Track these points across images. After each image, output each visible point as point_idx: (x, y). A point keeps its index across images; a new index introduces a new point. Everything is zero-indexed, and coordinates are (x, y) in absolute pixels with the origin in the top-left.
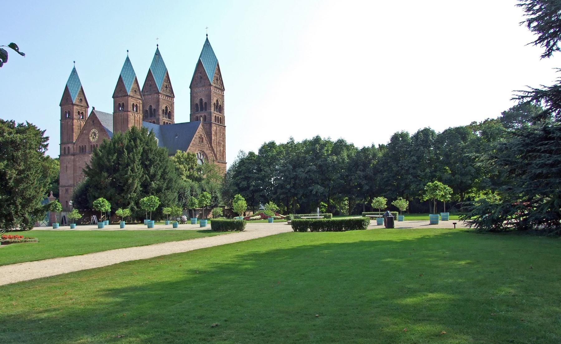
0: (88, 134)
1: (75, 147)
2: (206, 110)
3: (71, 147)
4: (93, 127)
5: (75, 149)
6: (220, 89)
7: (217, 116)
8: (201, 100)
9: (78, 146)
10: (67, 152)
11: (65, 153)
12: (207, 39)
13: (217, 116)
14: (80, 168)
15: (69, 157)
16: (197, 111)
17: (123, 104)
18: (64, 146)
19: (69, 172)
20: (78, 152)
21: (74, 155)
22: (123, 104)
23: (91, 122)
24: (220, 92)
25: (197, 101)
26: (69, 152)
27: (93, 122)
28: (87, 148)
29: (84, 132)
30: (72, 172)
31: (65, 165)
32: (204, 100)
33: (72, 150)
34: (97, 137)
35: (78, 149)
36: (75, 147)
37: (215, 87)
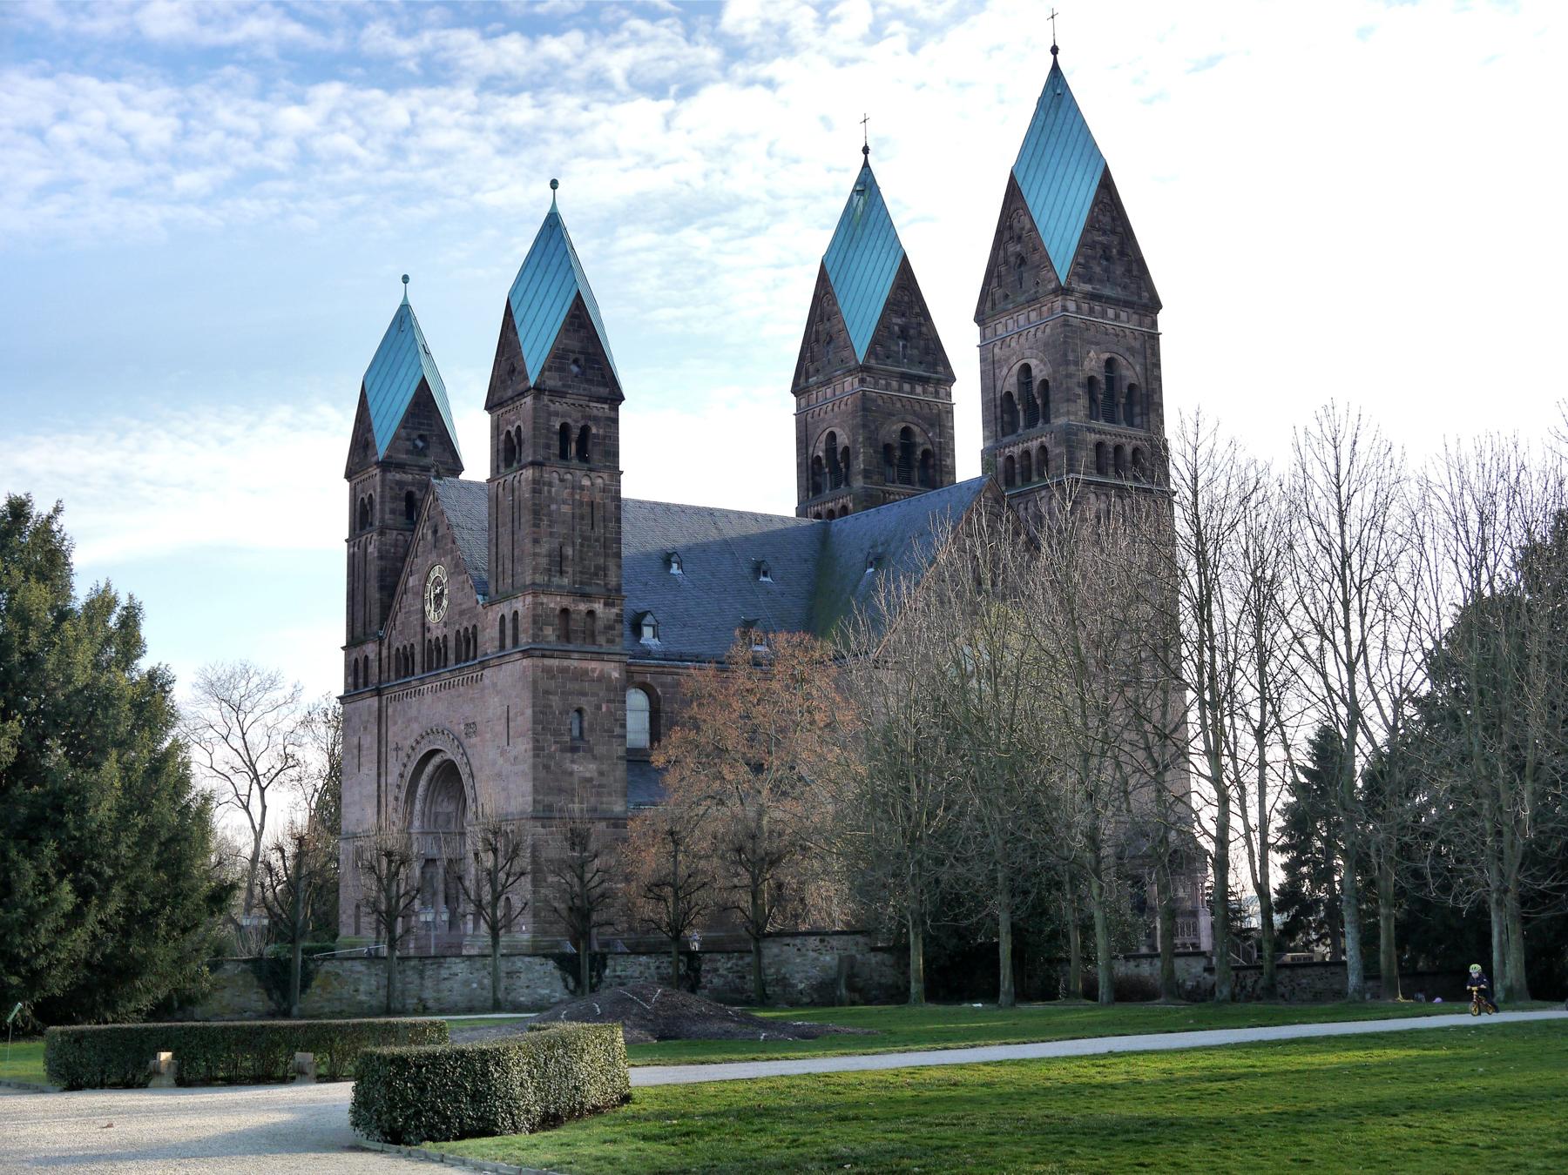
1: (385, 653)
2: (1047, 421)
3: (372, 656)
4: (433, 557)
6: (1127, 304)
7: (1110, 441)
8: (1026, 369)
9: (393, 652)
13: (1110, 441)
19: (364, 770)
24: (1129, 322)
25: (1010, 383)
27: (435, 532)
32: (1039, 372)
36: (385, 653)
37: (1093, 297)
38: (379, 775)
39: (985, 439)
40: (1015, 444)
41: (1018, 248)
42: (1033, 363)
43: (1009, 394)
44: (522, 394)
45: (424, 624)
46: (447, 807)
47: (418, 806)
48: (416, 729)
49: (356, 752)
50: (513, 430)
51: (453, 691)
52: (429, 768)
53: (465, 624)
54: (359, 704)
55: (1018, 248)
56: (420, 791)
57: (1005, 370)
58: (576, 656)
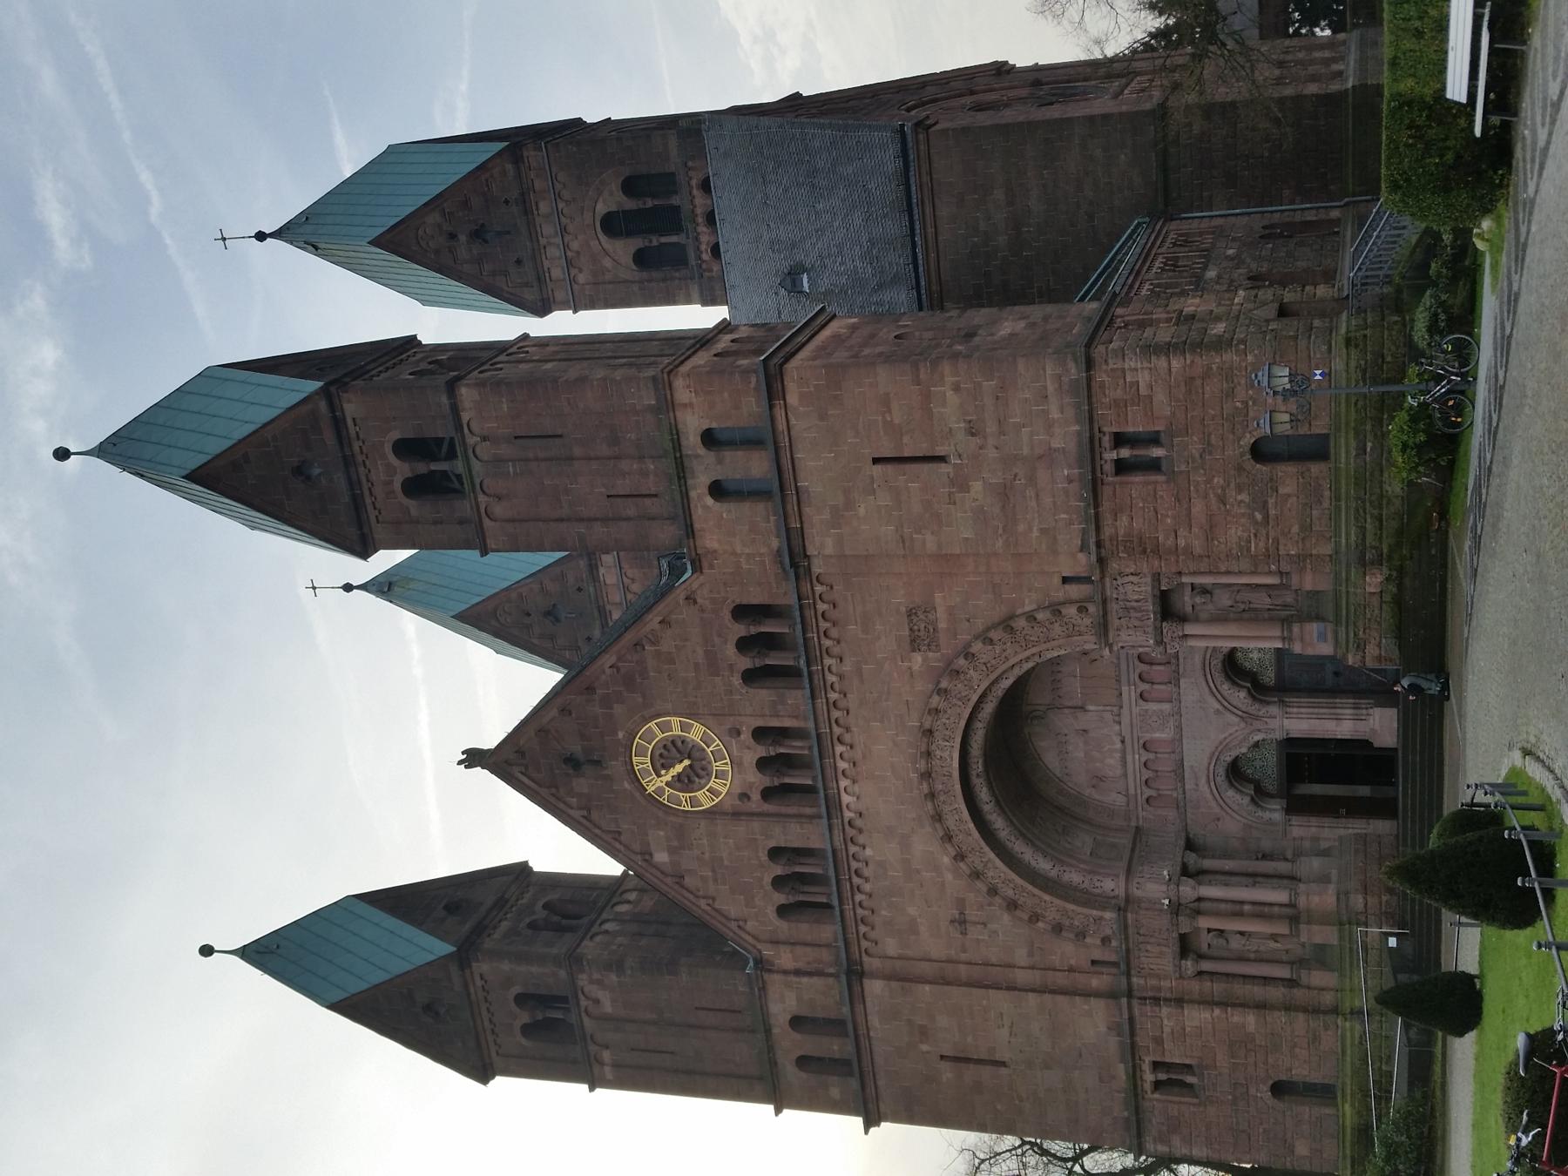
0: (680, 824)
4: (615, 767)
5: (805, 957)
9: (783, 927)
10: (834, 1047)
11: (839, 1066)
12: (278, 234)
14: (961, 922)
15: (874, 1021)
16: (681, 248)
17: (405, 448)
18: (791, 1073)
20: (828, 931)
21: (854, 974)
22: (405, 448)
23: (582, 784)
25: (622, 250)
26: (835, 1026)
28: (795, 835)
29: (661, 857)
30: (1000, 1001)
31: (947, 1072)
32: (611, 200)
33: (822, 995)
34: (696, 732)
35: (803, 929)
38: (1011, 988)
39: (688, 302)
40: (697, 239)
41: (463, 238)
42: (601, 209)
43: (642, 259)
44: (338, 423)
45: (736, 815)
46: (1083, 841)
47: (1074, 877)
48: (924, 843)
49: (970, 1073)
50: (404, 469)
51: (852, 701)
52: (998, 823)
53: (731, 650)
54: (879, 1060)
55: (463, 238)
56: (1043, 865)
57: (607, 262)
58: (801, 339)
